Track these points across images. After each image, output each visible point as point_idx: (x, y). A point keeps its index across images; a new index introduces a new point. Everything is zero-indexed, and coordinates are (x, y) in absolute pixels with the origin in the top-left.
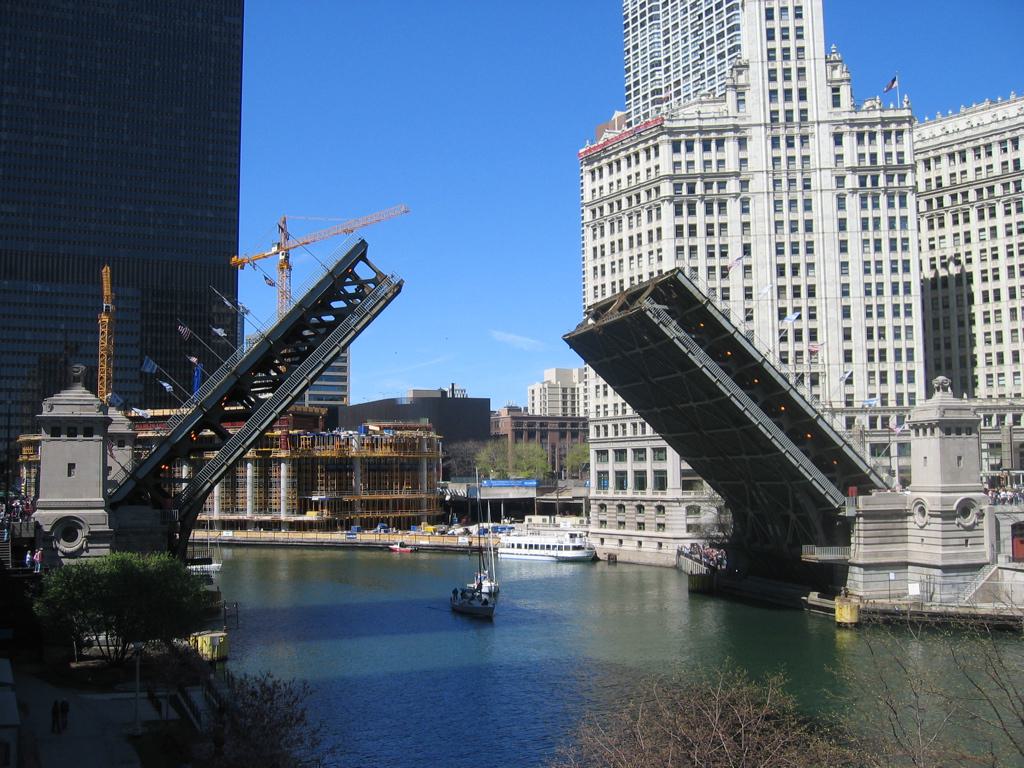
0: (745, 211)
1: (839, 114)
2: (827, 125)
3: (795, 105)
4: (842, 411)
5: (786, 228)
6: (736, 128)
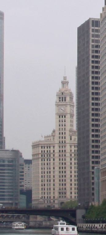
1: (71, 142)
3: (64, 140)
5: (61, 164)
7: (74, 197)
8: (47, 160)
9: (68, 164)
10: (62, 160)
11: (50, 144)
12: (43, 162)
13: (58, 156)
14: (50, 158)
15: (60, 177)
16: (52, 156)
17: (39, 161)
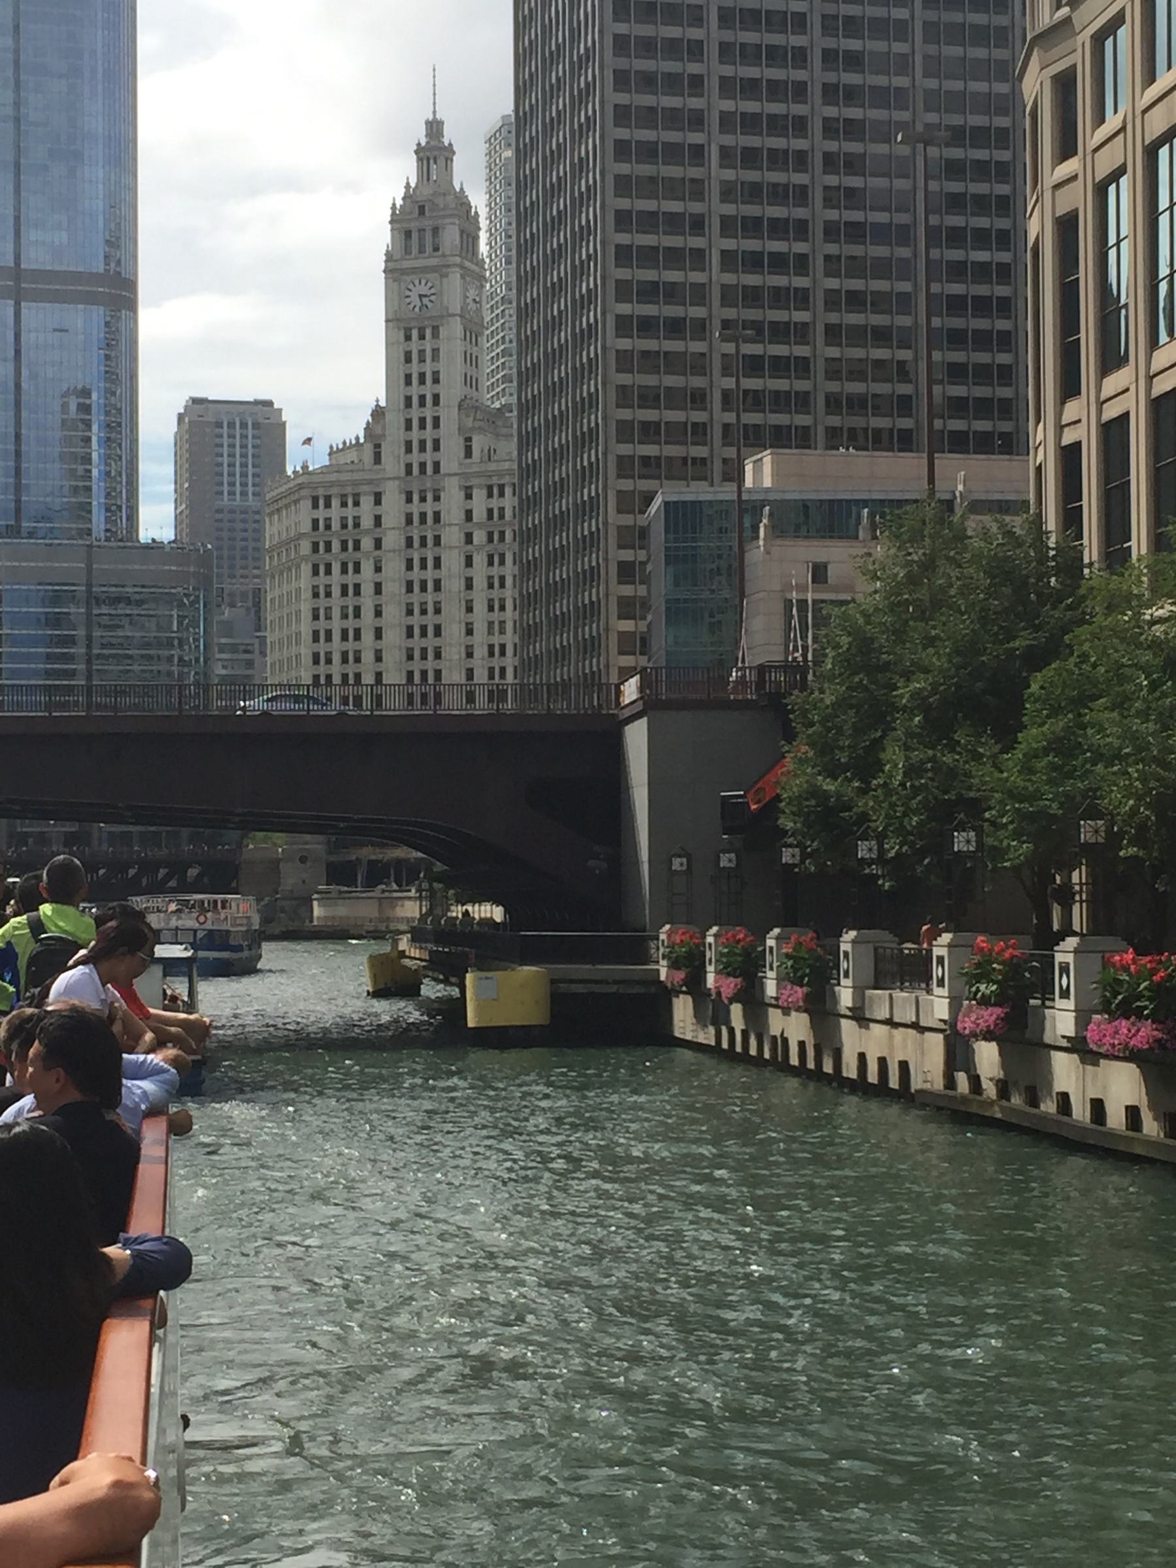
0: (378, 569)
2: (457, 478)
3: (429, 457)
5: (416, 588)
6: (370, 482)
8: (344, 571)
9: (453, 585)
10: (423, 566)
11: (356, 483)
12: (322, 579)
14: (358, 555)
15: (410, 657)
16: (367, 543)
17: (298, 578)
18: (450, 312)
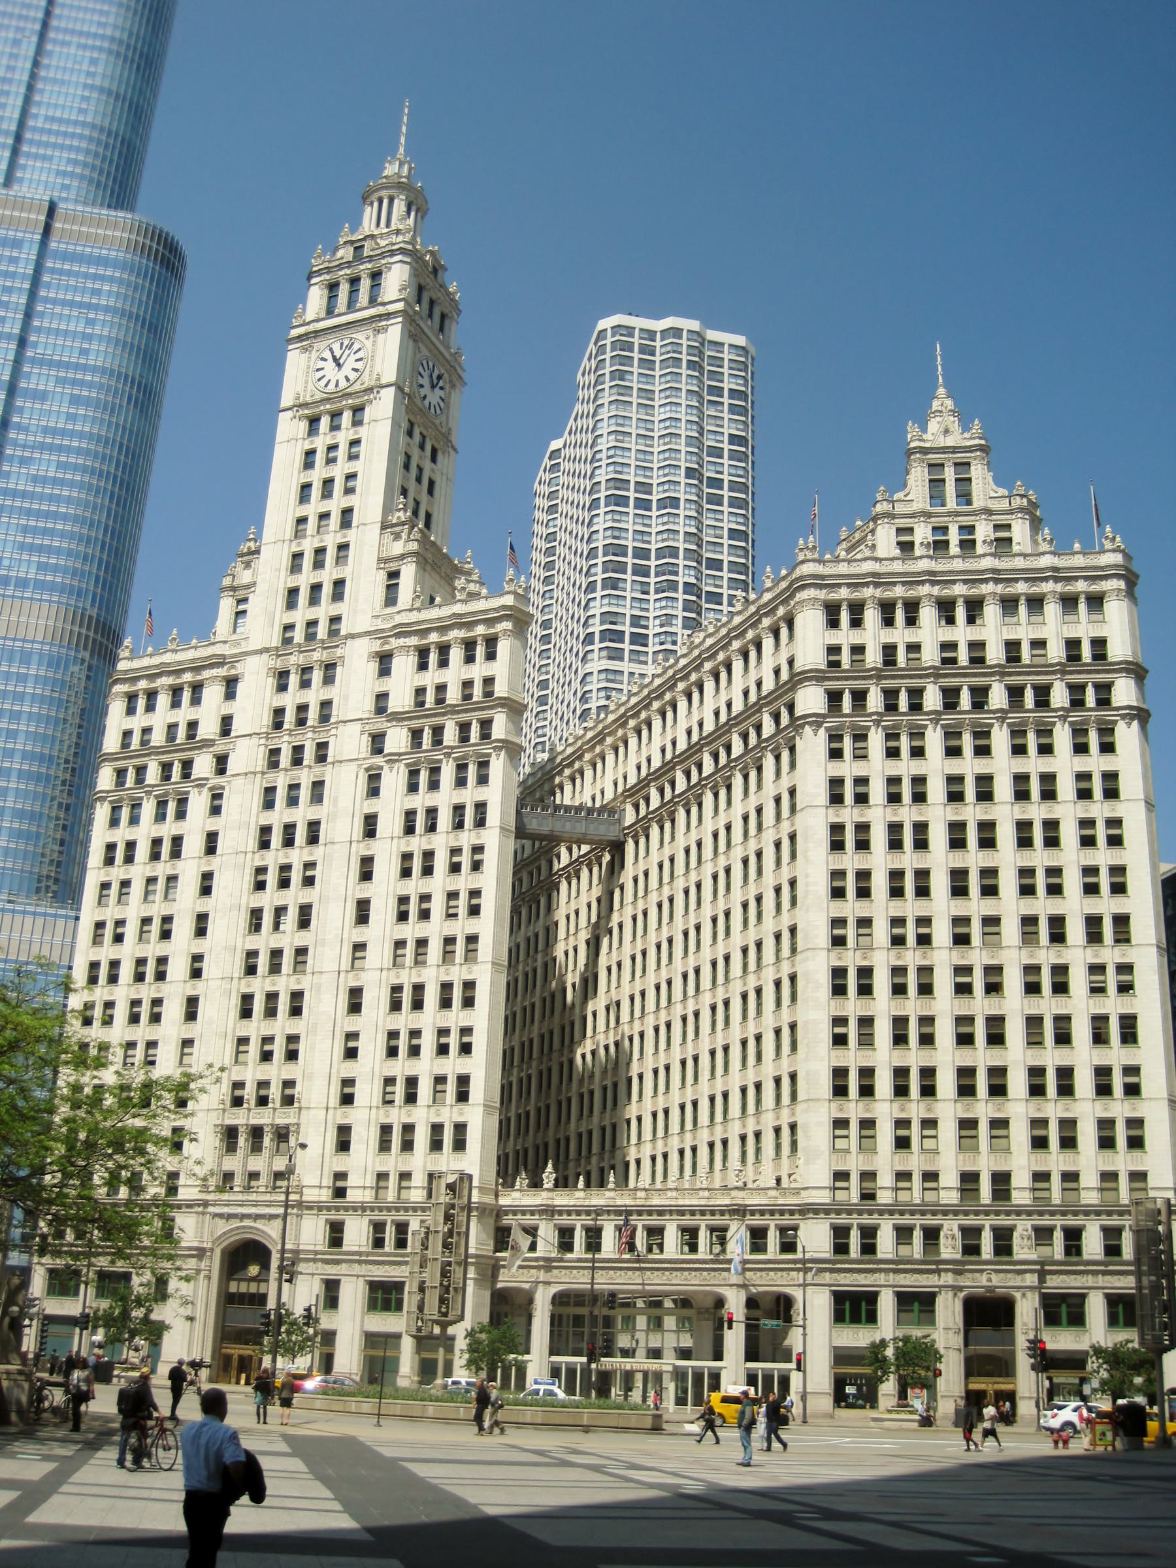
0: (216, 810)
3: (323, 612)
4: (319, 1207)
7: (370, 1180)
13: (261, 761)
14: (185, 787)
16: (203, 765)
18: (384, 381)
